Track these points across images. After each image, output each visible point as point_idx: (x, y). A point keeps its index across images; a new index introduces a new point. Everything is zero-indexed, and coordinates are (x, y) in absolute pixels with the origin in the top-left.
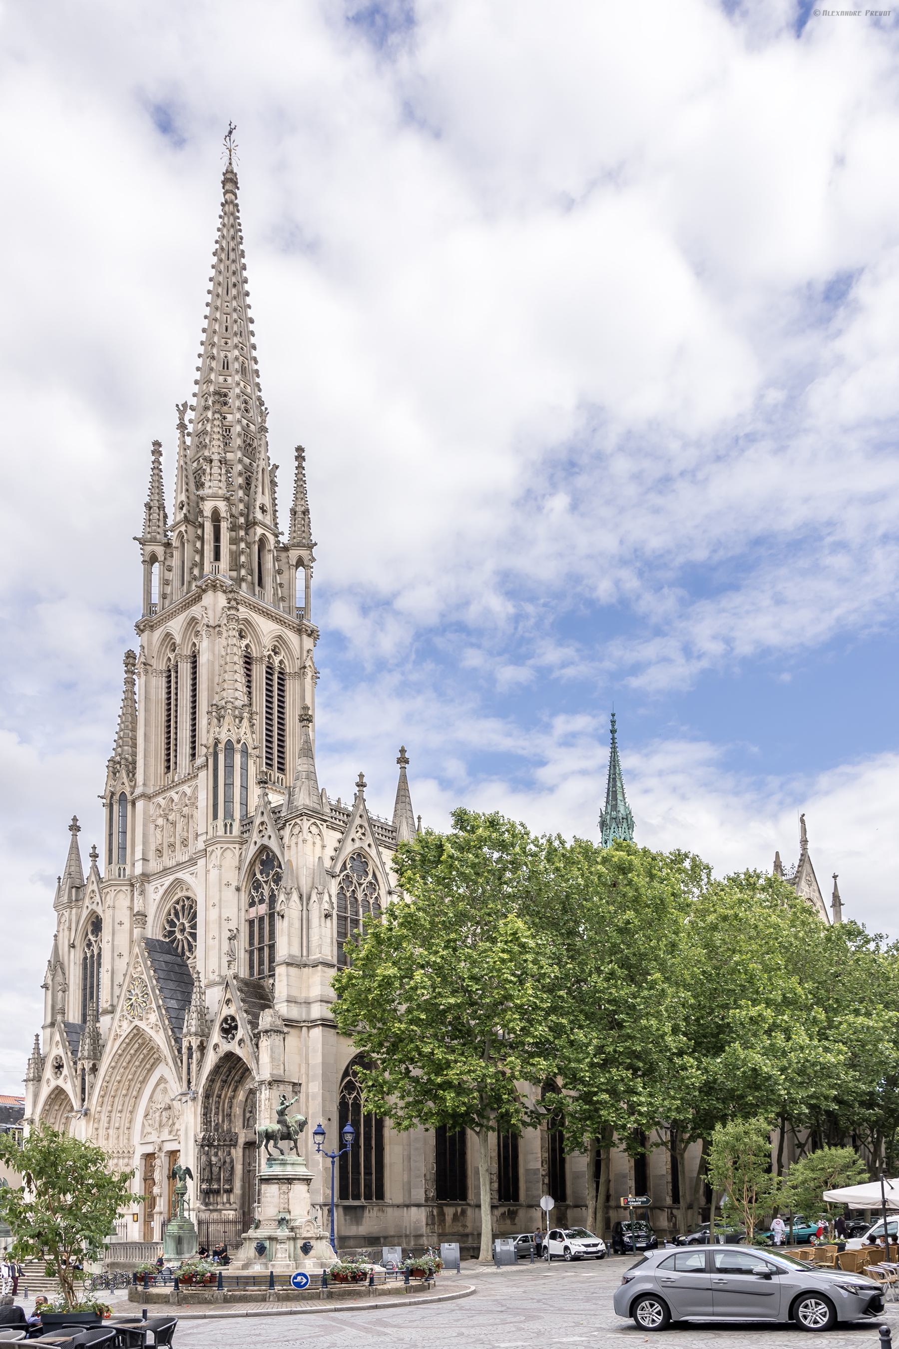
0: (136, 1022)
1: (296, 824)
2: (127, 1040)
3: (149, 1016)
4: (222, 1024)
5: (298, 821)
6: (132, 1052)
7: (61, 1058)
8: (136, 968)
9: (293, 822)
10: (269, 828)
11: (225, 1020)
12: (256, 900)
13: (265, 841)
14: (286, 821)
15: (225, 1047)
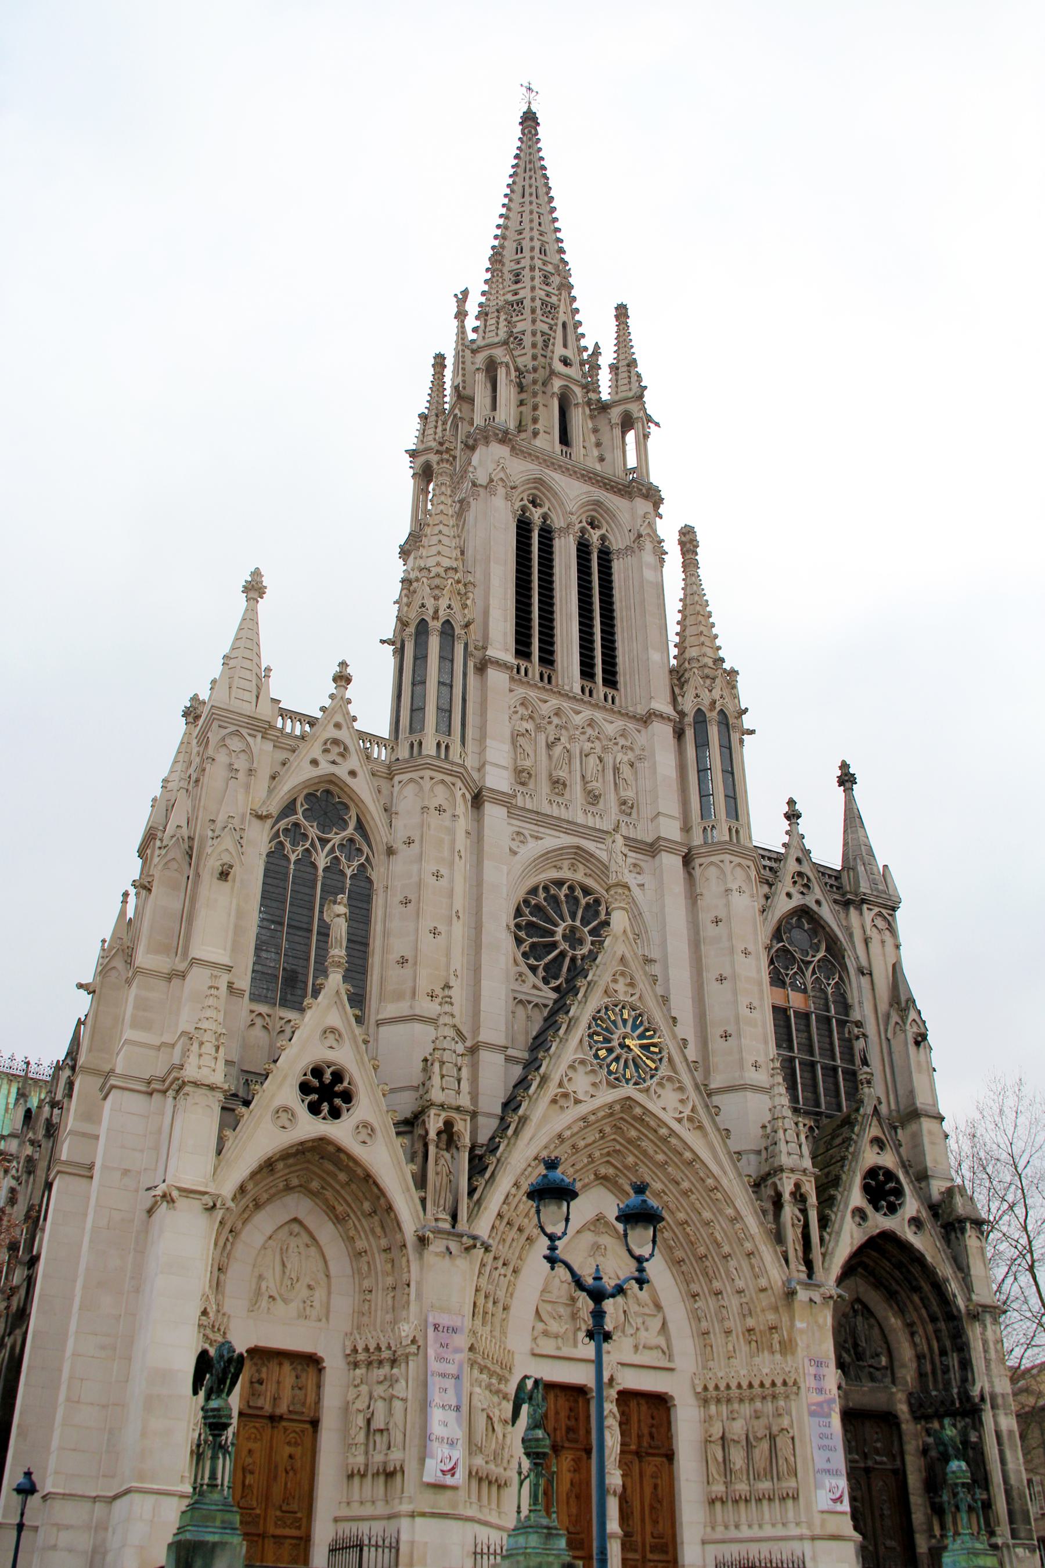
0: (628, 1090)
1: (880, 914)
2: (592, 1118)
3: (659, 1091)
4: (865, 1178)
5: (884, 911)
6: (582, 1144)
7: (338, 1076)
8: (615, 981)
9: (876, 910)
10: (817, 889)
11: (872, 1172)
12: (788, 980)
13: (810, 901)
14: (863, 901)
15: (879, 1222)
